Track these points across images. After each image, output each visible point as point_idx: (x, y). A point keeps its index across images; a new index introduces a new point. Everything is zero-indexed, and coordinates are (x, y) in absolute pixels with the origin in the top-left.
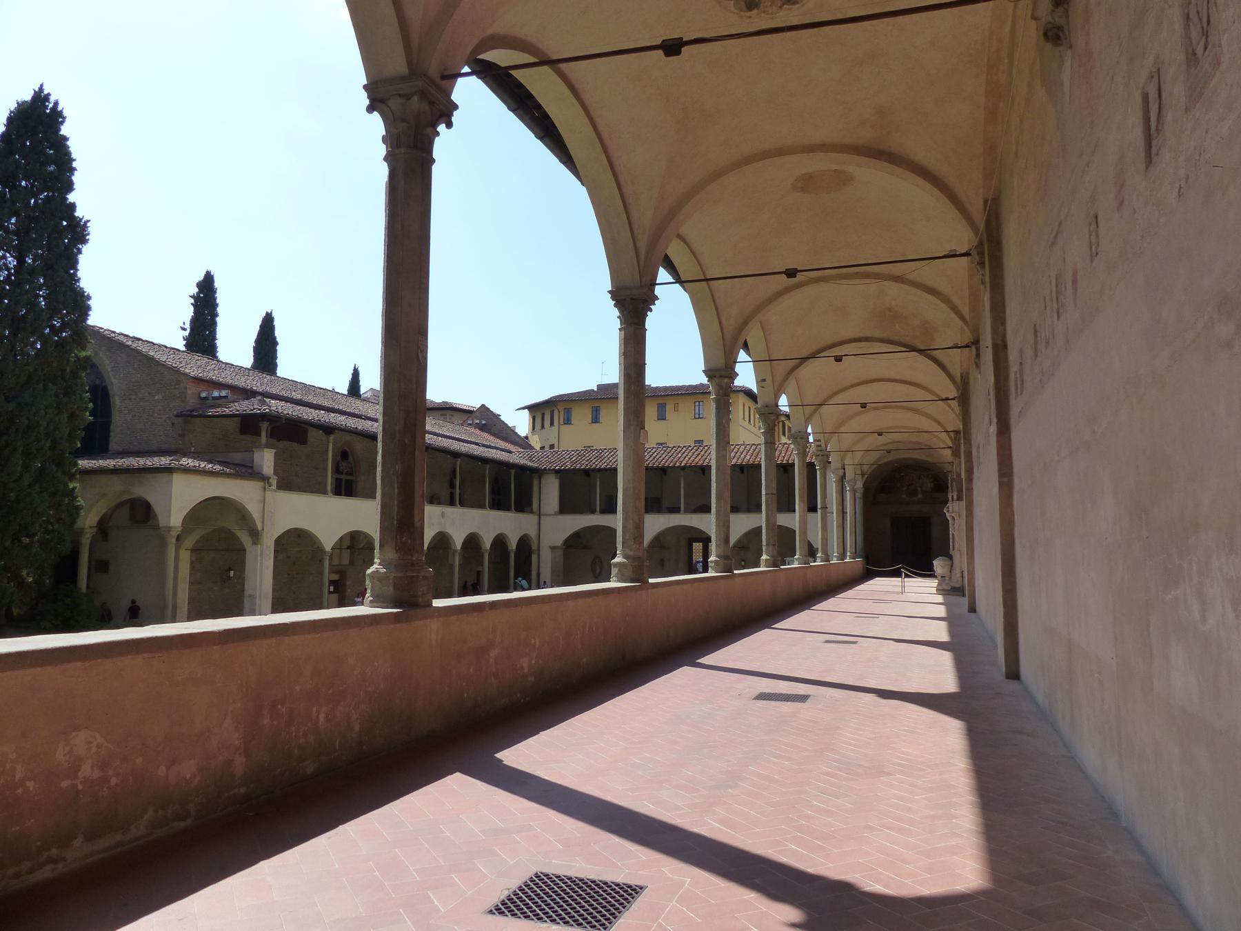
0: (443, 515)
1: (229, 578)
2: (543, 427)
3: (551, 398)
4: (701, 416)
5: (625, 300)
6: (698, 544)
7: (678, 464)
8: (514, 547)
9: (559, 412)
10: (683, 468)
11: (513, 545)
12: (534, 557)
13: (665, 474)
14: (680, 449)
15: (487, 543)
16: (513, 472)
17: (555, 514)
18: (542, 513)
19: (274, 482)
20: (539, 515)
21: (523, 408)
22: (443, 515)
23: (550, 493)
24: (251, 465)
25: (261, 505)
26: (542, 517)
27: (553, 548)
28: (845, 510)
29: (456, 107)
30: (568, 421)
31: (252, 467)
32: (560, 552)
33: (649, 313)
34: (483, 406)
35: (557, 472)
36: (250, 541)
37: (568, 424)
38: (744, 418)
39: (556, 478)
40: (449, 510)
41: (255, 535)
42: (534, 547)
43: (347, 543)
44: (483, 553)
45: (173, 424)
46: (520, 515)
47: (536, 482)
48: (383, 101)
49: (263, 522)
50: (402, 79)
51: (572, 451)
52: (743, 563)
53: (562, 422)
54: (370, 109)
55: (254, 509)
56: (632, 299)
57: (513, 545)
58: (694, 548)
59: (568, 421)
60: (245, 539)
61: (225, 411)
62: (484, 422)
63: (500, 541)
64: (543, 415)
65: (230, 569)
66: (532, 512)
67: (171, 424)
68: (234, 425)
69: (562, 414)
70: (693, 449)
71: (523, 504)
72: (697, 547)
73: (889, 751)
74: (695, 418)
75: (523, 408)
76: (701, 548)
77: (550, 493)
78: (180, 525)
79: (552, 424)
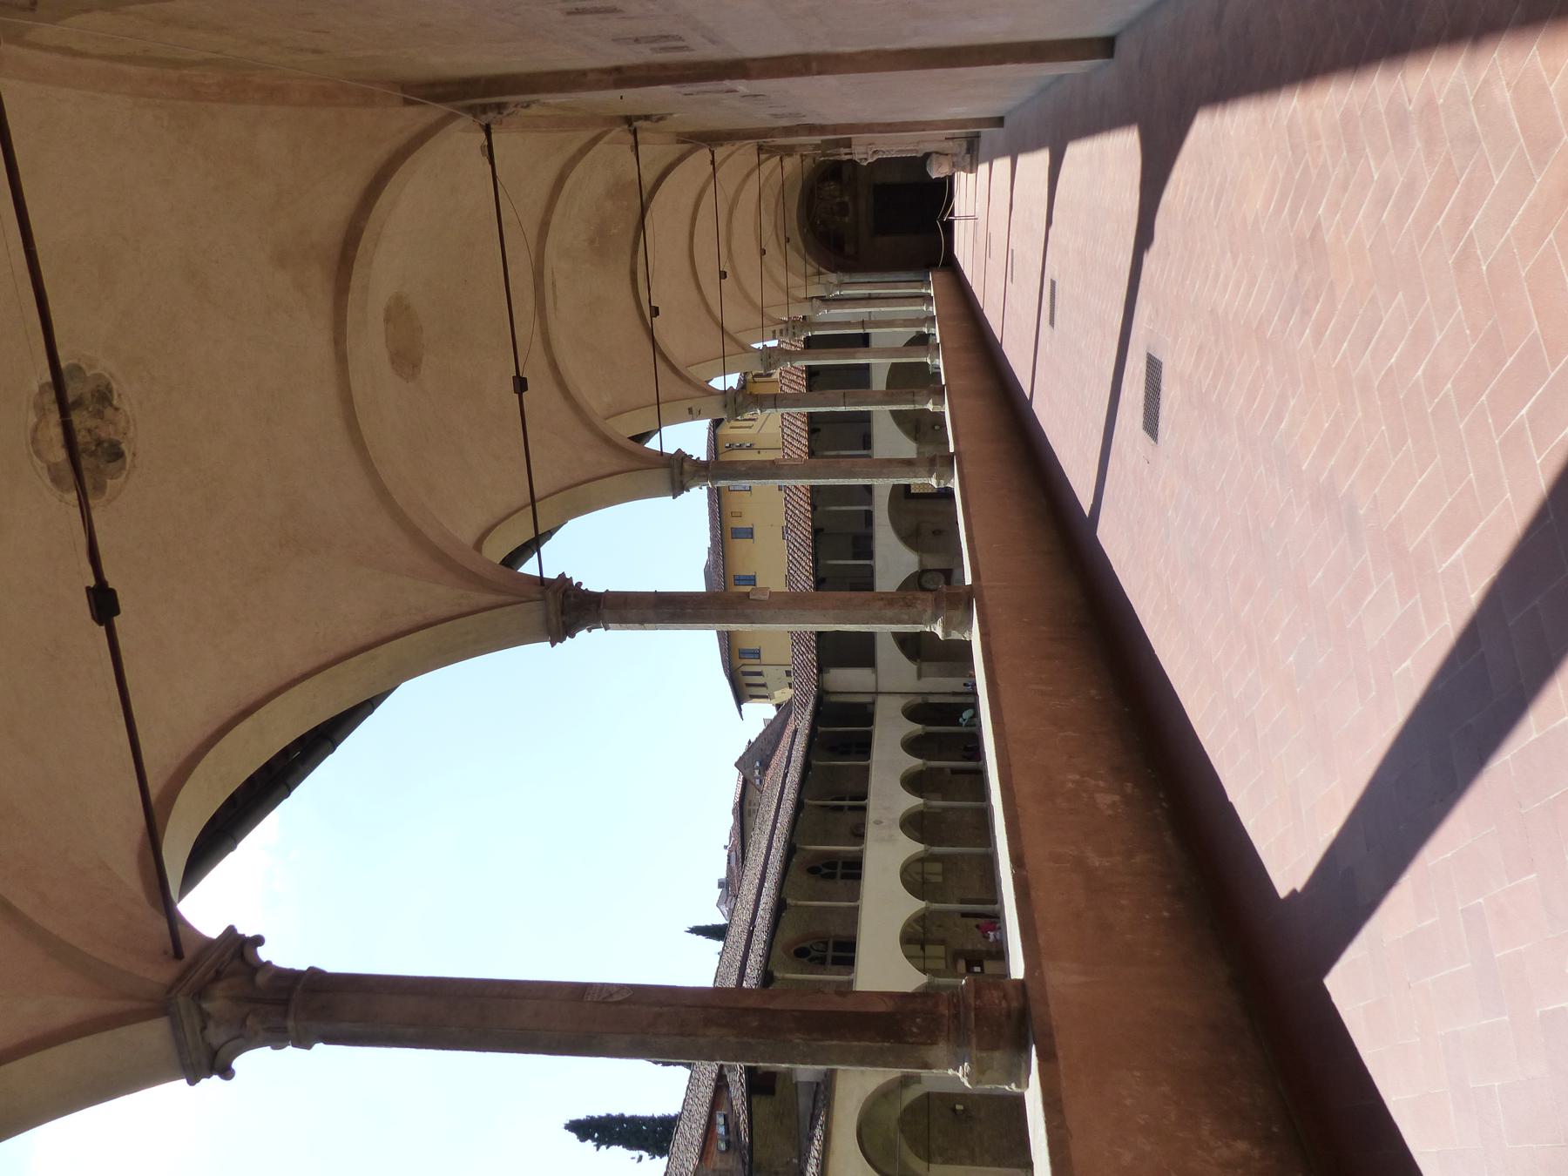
0: (878, 823)
1: (964, 1111)
2: (764, 685)
3: (726, 675)
5: (564, 622)
10: (814, 507)
12: (932, 700)
13: (822, 530)
14: (789, 512)
15: (912, 802)
16: (821, 729)
17: (876, 672)
18: (874, 690)
20: (877, 693)
21: (740, 710)
22: (878, 823)
24: (815, 1085)
27: (920, 676)
28: (867, 296)
29: (231, 930)
30: (756, 654)
31: (818, 1084)
32: (925, 665)
33: (583, 588)
34: (737, 765)
35: (820, 670)
37: (759, 654)
38: (750, 427)
40: (872, 815)
42: (919, 700)
43: (916, 949)
46: (878, 719)
47: (834, 699)
48: (214, 1054)
50: (176, 1026)
51: (793, 651)
52: (937, 427)
53: (757, 661)
54: (227, 1073)
56: (562, 613)
57: (916, 728)
58: (917, 491)
59: (756, 654)
62: (758, 764)
64: (749, 685)
65: (954, 1110)
66: (873, 703)
68: (763, 1105)
69: (746, 661)
70: (789, 495)
71: (863, 714)
73: (1263, 231)
75: (740, 710)
77: (848, 680)
79: (760, 674)
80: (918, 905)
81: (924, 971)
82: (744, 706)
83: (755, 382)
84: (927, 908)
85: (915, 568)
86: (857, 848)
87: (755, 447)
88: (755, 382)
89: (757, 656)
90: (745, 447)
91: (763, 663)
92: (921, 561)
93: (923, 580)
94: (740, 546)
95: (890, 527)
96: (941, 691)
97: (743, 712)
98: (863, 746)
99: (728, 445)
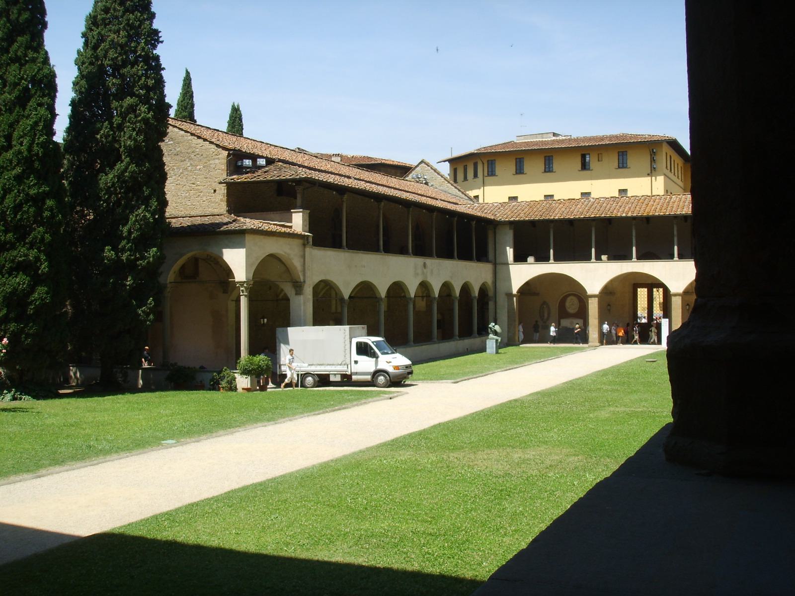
0: (425, 265)
2: (465, 179)
4: (625, 165)
6: (642, 289)
7: (630, 215)
8: (477, 295)
9: (483, 164)
12: (491, 305)
18: (498, 261)
19: (311, 240)
20: (495, 264)
22: (425, 265)
25: (302, 260)
26: (497, 266)
35: (511, 223)
36: (293, 292)
38: (667, 167)
39: (510, 229)
40: (429, 262)
41: (298, 287)
42: (491, 294)
45: (215, 191)
49: (304, 275)
55: (297, 263)
60: (289, 290)
61: (266, 178)
63: (466, 288)
66: (487, 261)
67: (213, 191)
72: (642, 293)
74: (619, 167)
75: (444, 161)
76: (646, 293)
78: (251, 279)
79: (476, 176)
80: (383, 293)
81: (350, 297)
82: (447, 162)
84: (381, 299)
85: (590, 291)
86: (411, 251)
89: (490, 173)
90: (653, 164)
91: (485, 178)
95: (620, 273)
97: (443, 163)
98: (465, 256)
99: (655, 151)
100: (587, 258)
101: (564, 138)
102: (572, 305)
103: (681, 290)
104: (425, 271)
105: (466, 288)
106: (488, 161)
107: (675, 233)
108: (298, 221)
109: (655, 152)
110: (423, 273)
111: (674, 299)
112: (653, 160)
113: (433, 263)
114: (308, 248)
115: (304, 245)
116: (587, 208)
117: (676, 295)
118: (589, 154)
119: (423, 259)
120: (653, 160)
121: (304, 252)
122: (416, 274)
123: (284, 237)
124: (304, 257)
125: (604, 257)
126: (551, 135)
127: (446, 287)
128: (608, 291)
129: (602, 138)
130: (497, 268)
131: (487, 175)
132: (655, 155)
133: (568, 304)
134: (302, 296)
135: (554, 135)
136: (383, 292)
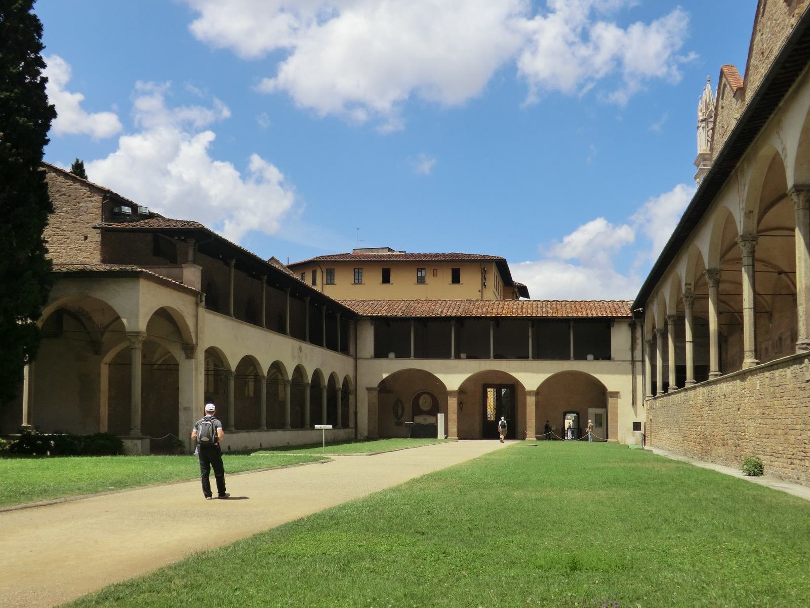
0: (300, 347)
7: (489, 315)
11: (340, 385)
17: (371, 358)
18: (358, 357)
20: (356, 359)
23: (367, 339)
25: (195, 320)
26: (358, 360)
36: (183, 355)
39: (371, 324)
41: (189, 350)
42: (351, 388)
44: (321, 390)
47: (352, 327)
49: (197, 337)
53: (325, 282)
55: (190, 322)
57: (340, 385)
60: (178, 354)
72: (491, 393)
77: (367, 339)
83: (513, 294)
84: (264, 377)
87: (484, 288)
88: (513, 294)
89: (329, 282)
90: (483, 281)
92: (452, 393)
93: (425, 395)
94: (412, 277)
96: (358, 404)
98: (332, 347)
100: (446, 355)
101: (399, 253)
102: (425, 403)
103: (535, 388)
104: (300, 354)
105: (332, 377)
106: (327, 269)
107: (530, 334)
108: (192, 276)
109: (485, 271)
110: (299, 357)
111: (528, 398)
112: (484, 278)
113: (307, 347)
114: (201, 308)
115: (197, 305)
116: (446, 309)
117: (530, 393)
118: (425, 269)
119: (299, 343)
120: (484, 278)
121: (197, 311)
122: (294, 357)
123: (179, 291)
124: (196, 317)
125: (463, 355)
126: (387, 250)
127: (317, 374)
128: (462, 391)
129: (436, 255)
130: (358, 362)
131: (325, 283)
132: (485, 273)
133: (421, 402)
134: (194, 360)
135: (390, 250)
136: (265, 368)
